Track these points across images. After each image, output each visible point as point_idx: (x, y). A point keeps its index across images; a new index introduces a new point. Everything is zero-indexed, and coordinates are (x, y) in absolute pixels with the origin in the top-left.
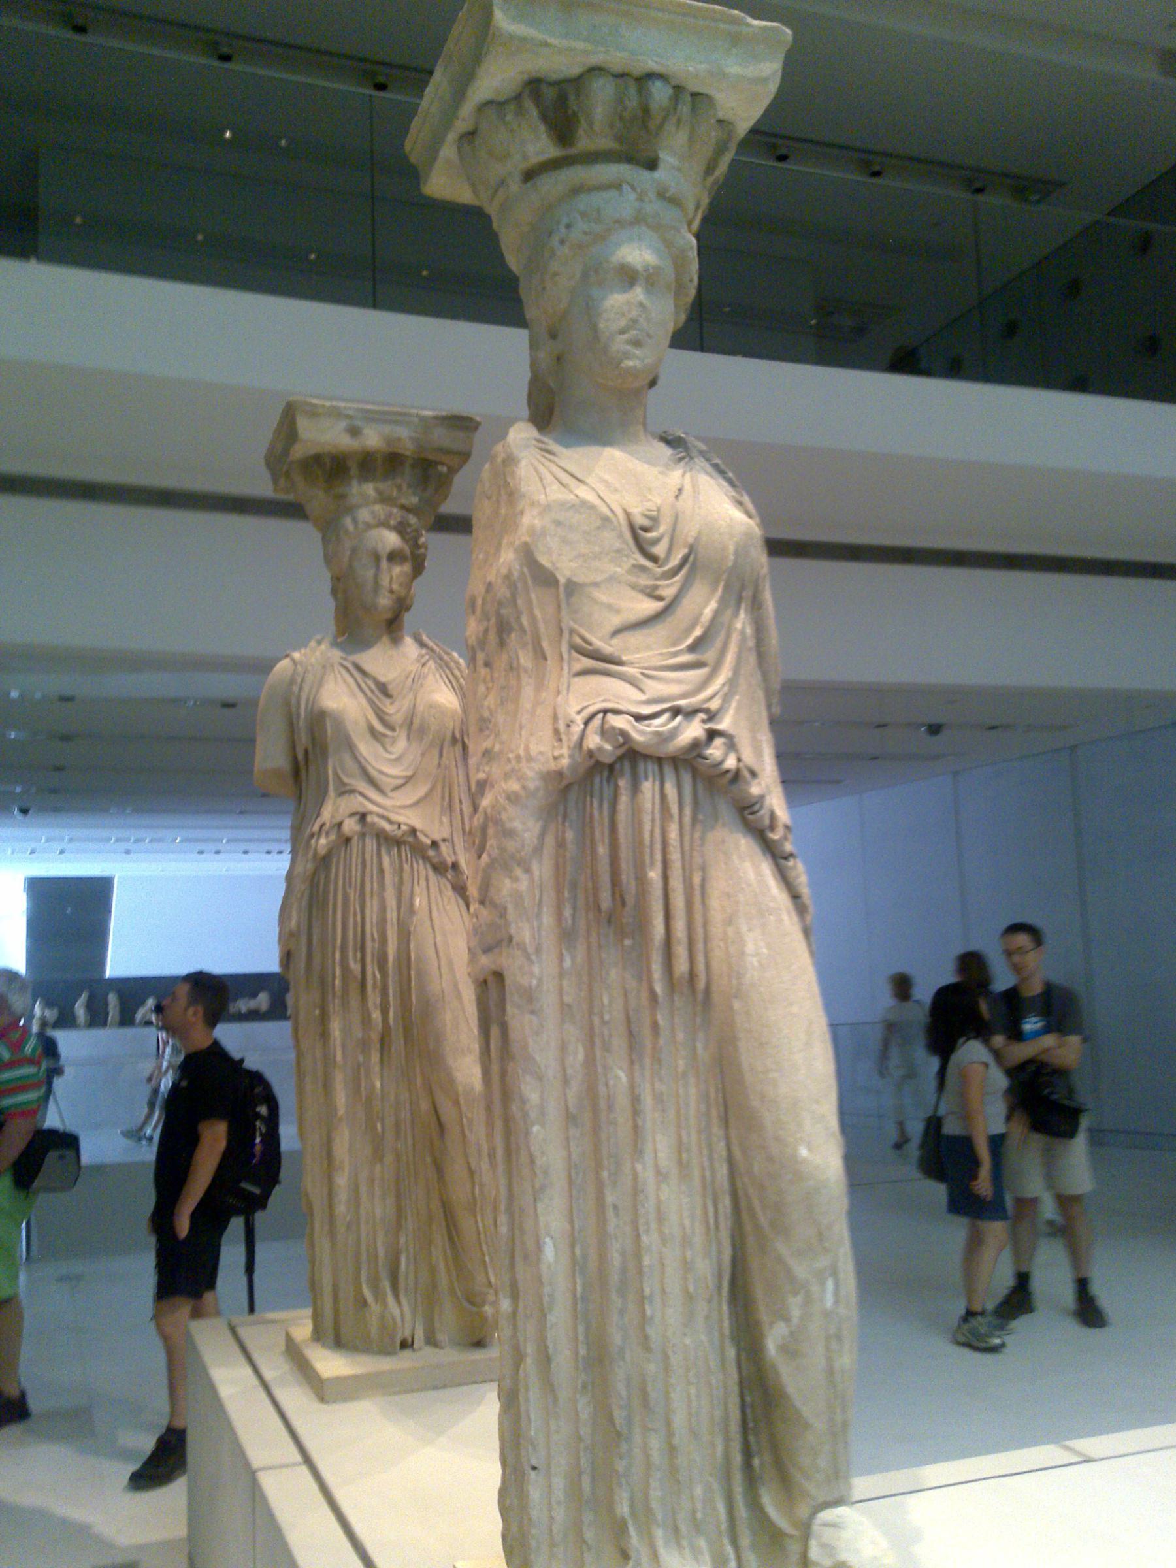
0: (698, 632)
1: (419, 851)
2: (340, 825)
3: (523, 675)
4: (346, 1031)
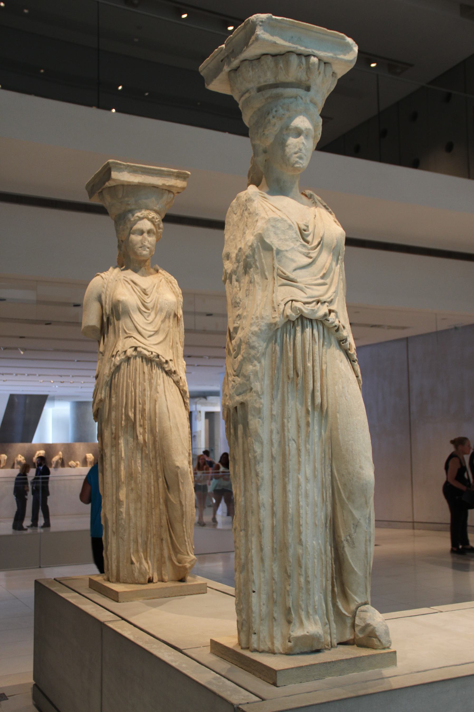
0: (324, 271)
1: (161, 365)
2: (125, 352)
3: (256, 285)
4: (127, 444)
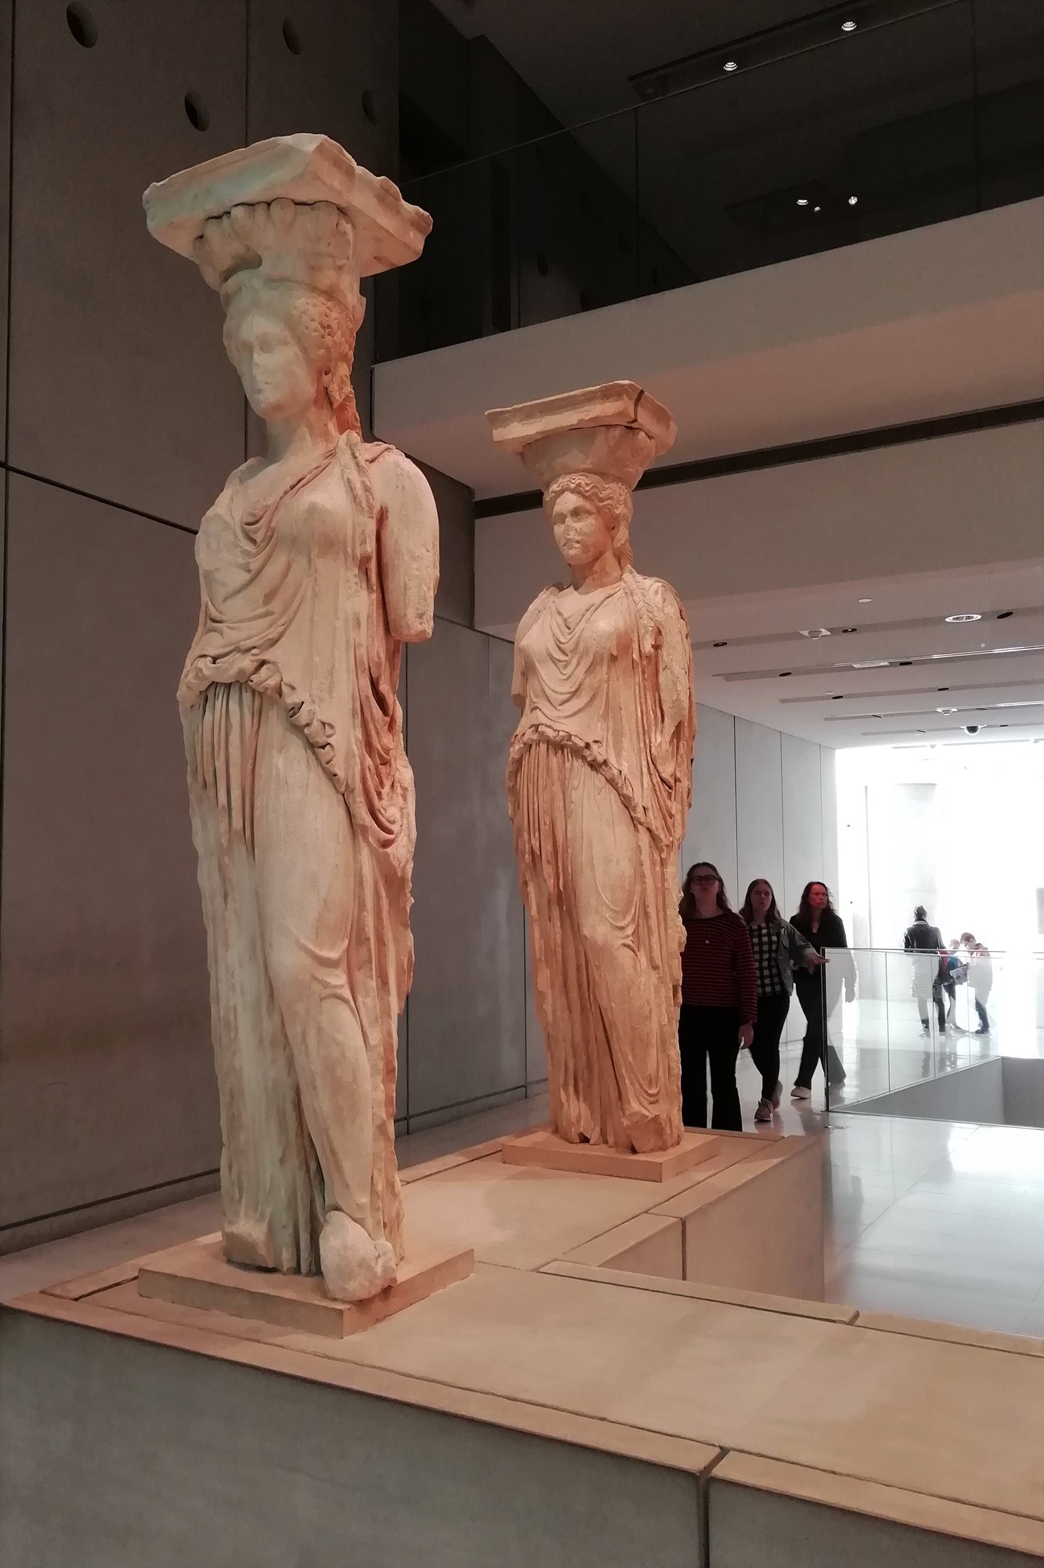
1: (578, 753)
